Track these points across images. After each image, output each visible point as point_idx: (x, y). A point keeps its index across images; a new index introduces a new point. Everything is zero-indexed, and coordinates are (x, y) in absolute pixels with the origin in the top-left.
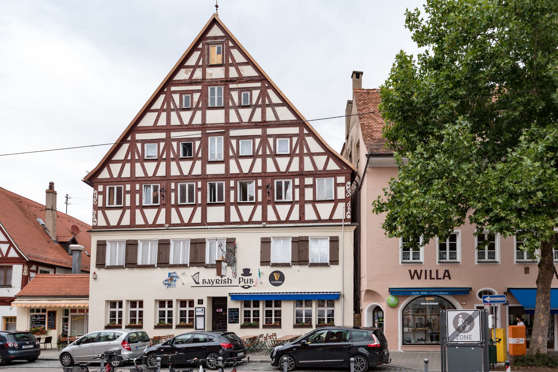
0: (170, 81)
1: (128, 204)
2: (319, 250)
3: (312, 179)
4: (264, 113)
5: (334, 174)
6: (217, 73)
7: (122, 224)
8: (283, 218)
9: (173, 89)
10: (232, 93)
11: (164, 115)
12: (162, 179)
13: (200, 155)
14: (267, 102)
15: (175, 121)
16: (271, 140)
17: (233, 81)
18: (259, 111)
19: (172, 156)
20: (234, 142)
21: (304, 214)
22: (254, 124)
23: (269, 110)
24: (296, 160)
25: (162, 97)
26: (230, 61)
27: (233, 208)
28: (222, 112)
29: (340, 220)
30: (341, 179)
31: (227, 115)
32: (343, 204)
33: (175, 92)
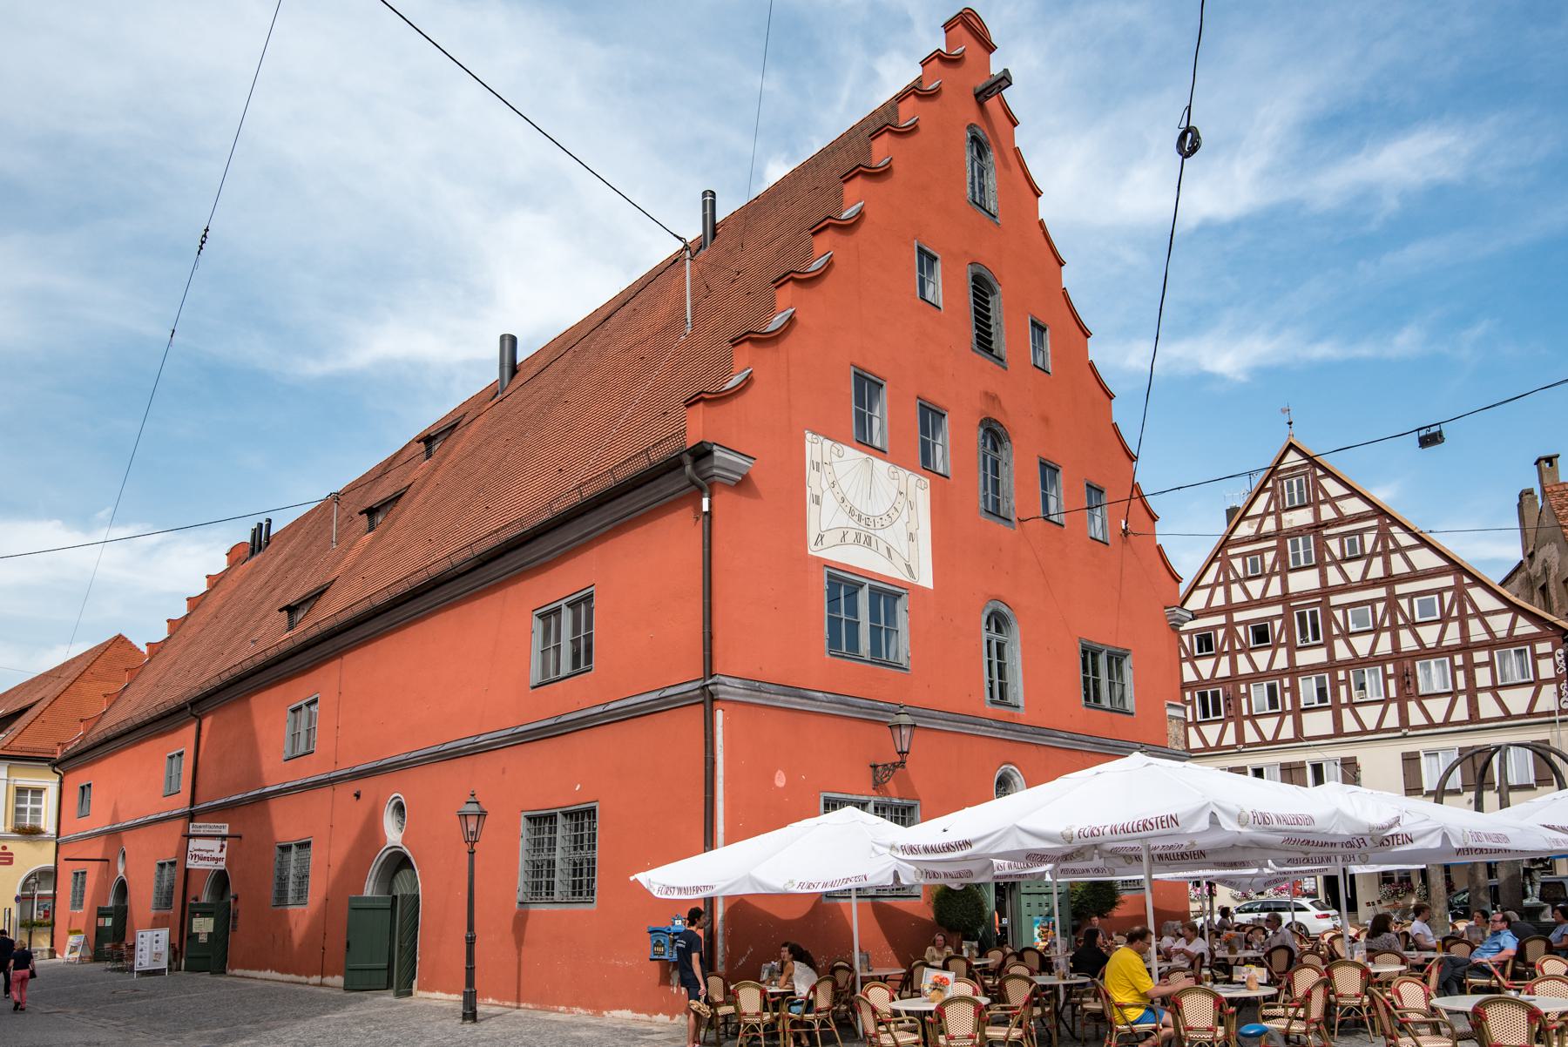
0: (1226, 543)
4: (1387, 564)
5: (1531, 640)
6: (1303, 517)
8: (1438, 718)
9: (1231, 552)
10: (1329, 542)
11: (1220, 591)
14: (1391, 546)
15: (1238, 596)
16: (1404, 603)
17: (1327, 525)
19: (1238, 647)
20: (1338, 614)
21: (1477, 709)
25: (1215, 566)
26: (1321, 497)
27: (1346, 713)
28: (1315, 572)
30: (1544, 647)
32: (1553, 687)
33: (1235, 556)
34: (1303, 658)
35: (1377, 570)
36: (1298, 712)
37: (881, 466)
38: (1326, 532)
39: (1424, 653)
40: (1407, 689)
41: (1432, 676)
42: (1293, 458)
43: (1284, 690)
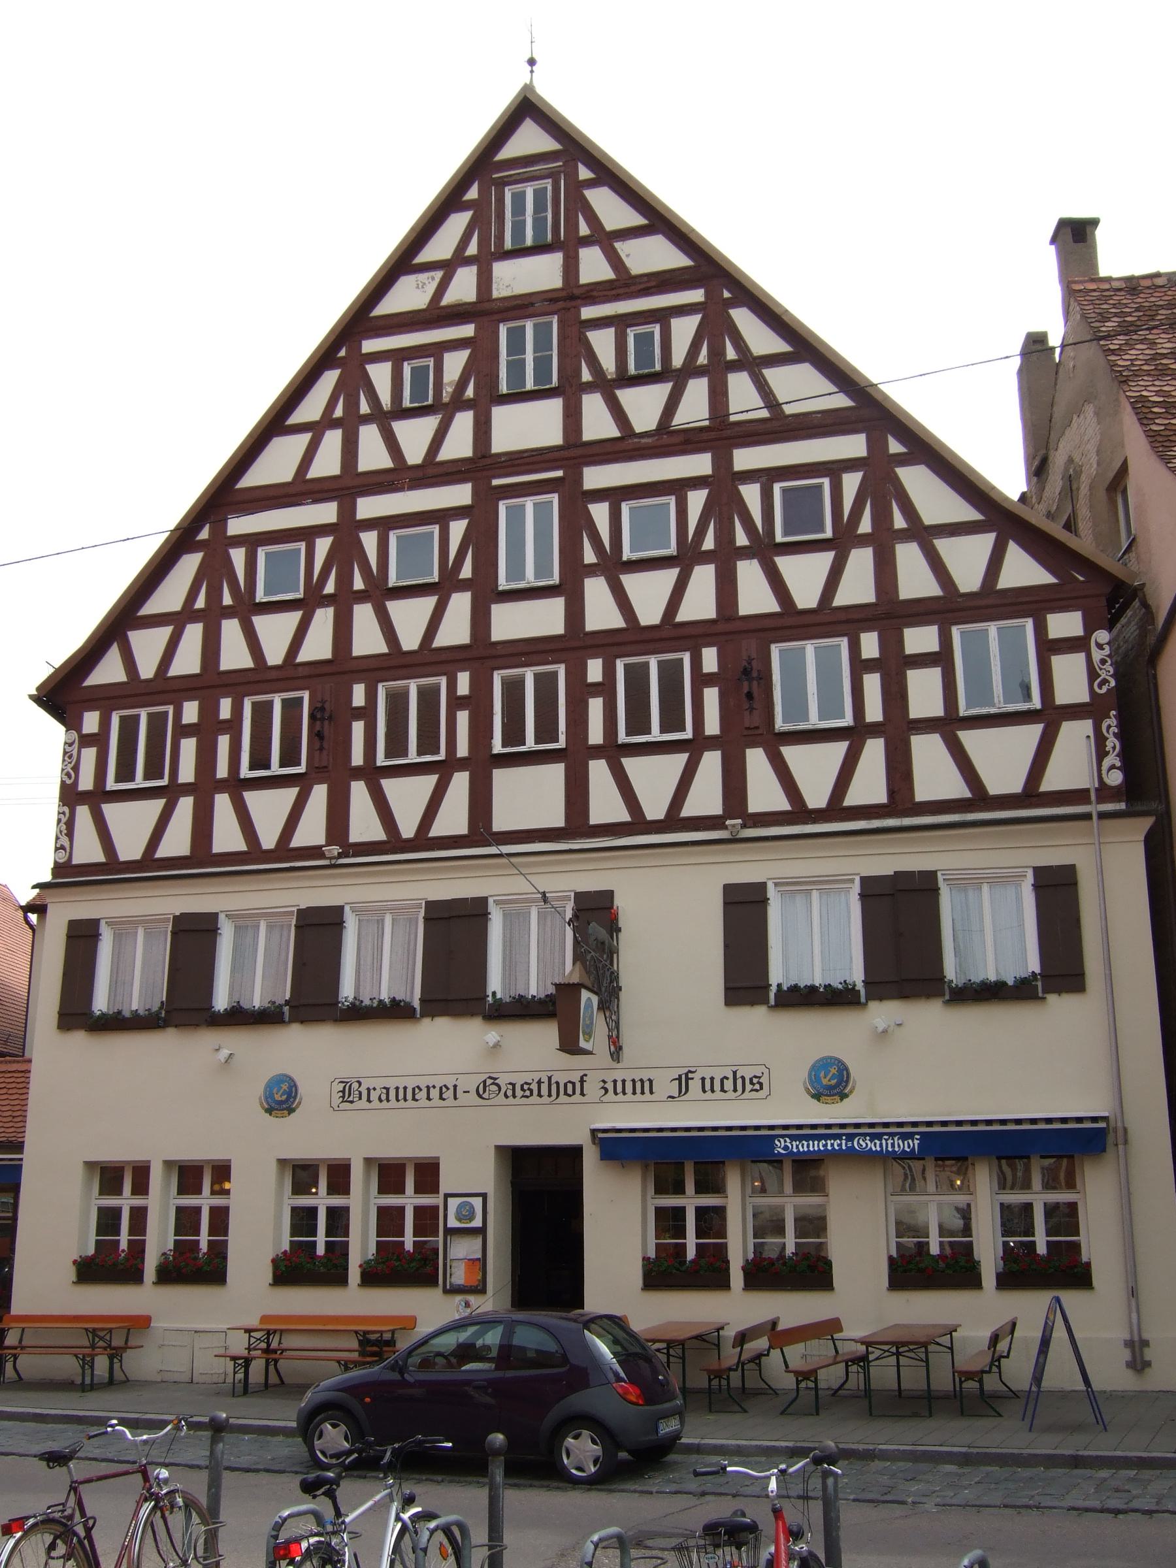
0: (360, 321)
1: (187, 774)
2: (990, 930)
3: (934, 629)
4: (718, 396)
6: (538, 274)
7: (162, 852)
8: (817, 797)
9: (370, 346)
11: (333, 440)
13: (466, 572)
14: (731, 354)
15: (373, 454)
16: (751, 494)
19: (359, 584)
20: (600, 513)
22: (681, 438)
25: (330, 379)
27: (598, 770)
29: (1078, 796)
30: (1065, 624)
31: (572, 418)
32: (1085, 727)
35: (694, 407)
36: (482, 766)
38: (588, 313)
41: (807, 677)
42: (530, 140)
43: (456, 702)
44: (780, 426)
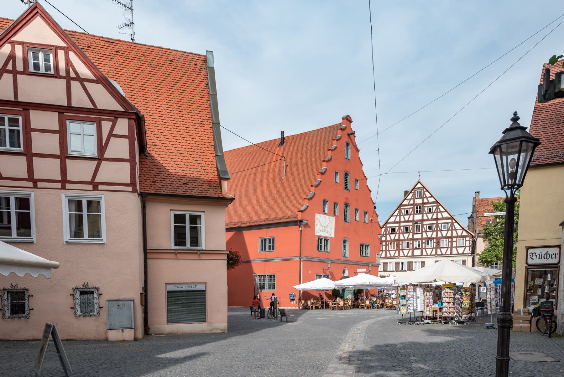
0: (401, 205)
1: (384, 249)
4: (437, 215)
5: (465, 237)
11: (398, 217)
12: (397, 240)
15: (402, 219)
16: (440, 225)
17: (425, 204)
18: (435, 214)
23: (439, 214)
24: (450, 232)
25: (398, 211)
27: (424, 250)
31: (423, 217)
34: (416, 236)
36: (413, 249)
37: (327, 216)
39: (443, 238)
40: (438, 246)
41: (444, 243)
42: (419, 185)
44: (443, 219)
